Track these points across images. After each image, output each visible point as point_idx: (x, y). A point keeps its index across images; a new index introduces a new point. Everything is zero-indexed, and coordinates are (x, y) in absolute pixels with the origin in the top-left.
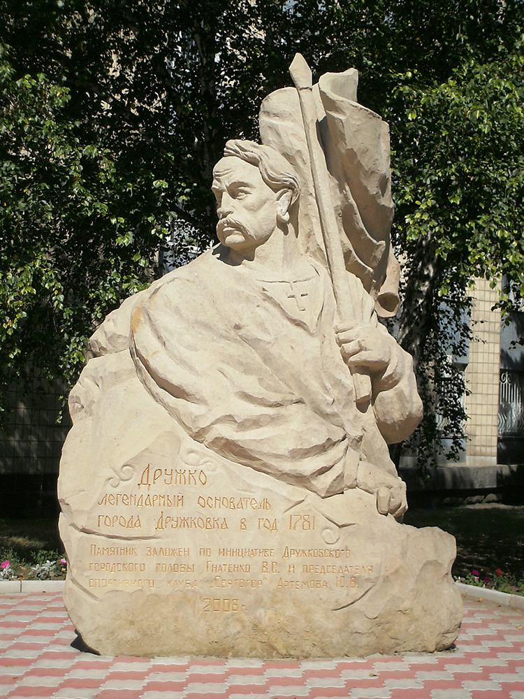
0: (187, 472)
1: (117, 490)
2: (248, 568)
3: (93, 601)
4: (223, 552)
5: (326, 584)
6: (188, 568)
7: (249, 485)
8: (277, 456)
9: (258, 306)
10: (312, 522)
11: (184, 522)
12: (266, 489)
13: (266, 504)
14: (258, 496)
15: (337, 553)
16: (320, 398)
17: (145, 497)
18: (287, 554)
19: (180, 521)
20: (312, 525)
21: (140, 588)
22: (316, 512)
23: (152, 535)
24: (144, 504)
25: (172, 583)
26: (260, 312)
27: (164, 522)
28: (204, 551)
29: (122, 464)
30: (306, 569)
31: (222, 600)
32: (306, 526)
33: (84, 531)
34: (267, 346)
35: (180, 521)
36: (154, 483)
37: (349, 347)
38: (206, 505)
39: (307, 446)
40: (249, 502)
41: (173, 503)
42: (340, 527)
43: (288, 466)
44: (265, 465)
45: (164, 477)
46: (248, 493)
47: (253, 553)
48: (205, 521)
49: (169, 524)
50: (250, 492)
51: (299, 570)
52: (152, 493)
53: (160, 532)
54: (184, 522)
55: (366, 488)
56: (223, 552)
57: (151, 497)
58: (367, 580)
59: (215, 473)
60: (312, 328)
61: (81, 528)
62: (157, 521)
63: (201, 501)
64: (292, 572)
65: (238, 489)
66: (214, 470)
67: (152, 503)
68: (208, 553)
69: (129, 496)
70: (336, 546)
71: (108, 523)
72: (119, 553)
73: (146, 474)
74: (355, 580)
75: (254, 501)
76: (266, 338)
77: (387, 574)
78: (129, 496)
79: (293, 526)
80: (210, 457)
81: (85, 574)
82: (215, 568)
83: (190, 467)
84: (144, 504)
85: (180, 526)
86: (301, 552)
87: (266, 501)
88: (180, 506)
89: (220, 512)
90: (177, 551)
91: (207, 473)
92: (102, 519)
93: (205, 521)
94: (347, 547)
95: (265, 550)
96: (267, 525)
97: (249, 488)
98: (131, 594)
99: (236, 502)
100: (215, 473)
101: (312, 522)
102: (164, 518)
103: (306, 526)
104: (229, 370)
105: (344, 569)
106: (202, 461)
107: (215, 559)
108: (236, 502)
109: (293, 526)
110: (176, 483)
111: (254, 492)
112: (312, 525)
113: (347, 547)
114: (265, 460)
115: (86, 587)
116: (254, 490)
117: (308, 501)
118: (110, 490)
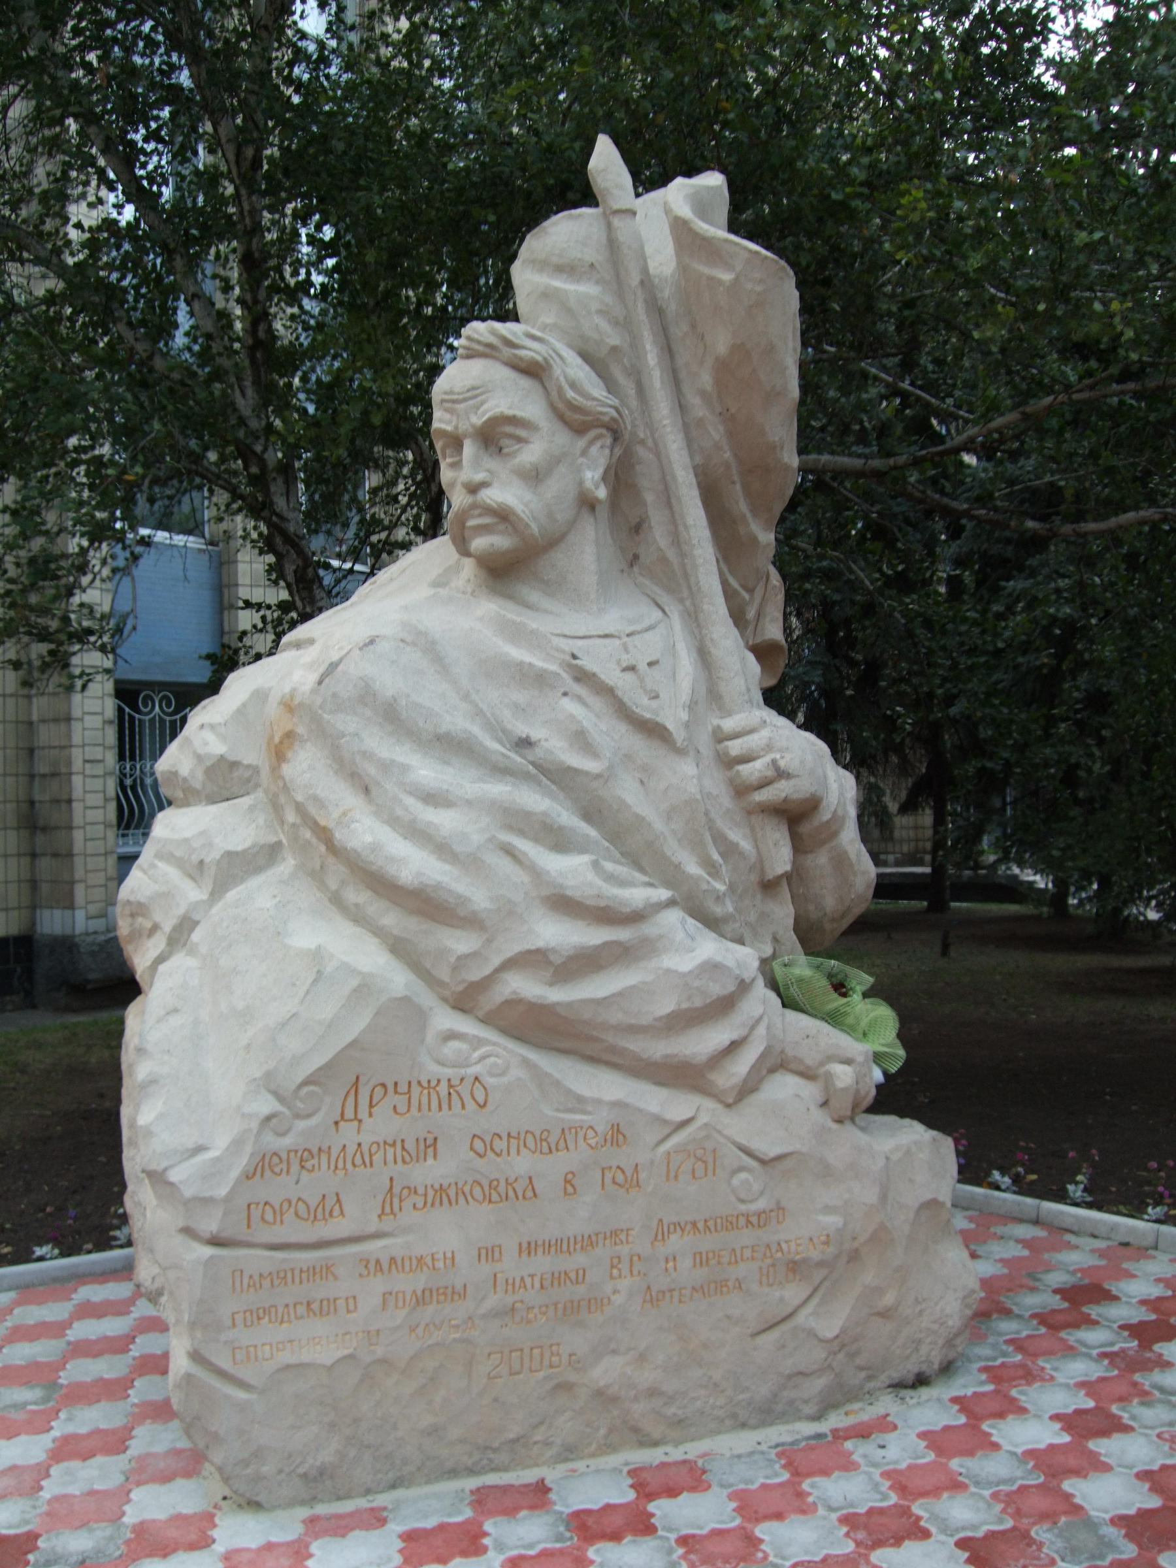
0: (444, 1084)
1: (287, 1141)
2: (580, 1276)
3: (242, 1395)
4: (529, 1248)
5: (739, 1284)
6: (457, 1294)
7: (580, 1099)
8: (634, 1030)
9: (565, 694)
10: (710, 1160)
11: (442, 1195)
12: (618, 1105)
13: (617, 1135)
14: (600, 1120)
15: (759, 1220)
16: (705, 886)
17: (352, 1147)
18: (662, 1232)
19: (431, 1193)
20: (710, 1168)
21: (350, 1351)
22: (722, 1140)
23: (372, 1228)
24: (349, 1165)
25: (420, 1330)
26: (569, 706)
27: (396, 1201)
28: (489, 1253)
29: (299, 1080)
30: (700, 1259)
31: (527, 1351)
32: (700, 1172)
33: (216, 1242)
34: (595, 784)
35: (431, 1193)
36: (371, 1115)
37: (753, 770)
38: (489, 1153)
39: (698, 1002)
40: (581, 1134)
41: (414, 1154)
42: (762, 1162)
43: (658, 1049)
44: (613, 1049)
45: (392, 1099)
46: (578, 1117)
47: (589, 1242)
48: (487, 1189)
49: (408, 1204)
50: (584, 1112)
51: (686, 1263)
52: (366, 1139)
53: (388, 1224)
54: (442, 1195)
55: (802, 1068)
56: (529, 1248)
57: (365, 1148)
58: (821, 1264)
59: (505, 1080)
60: (679, 735)
61: (207, 1235)
62: (380, 1198)
63: (478, 1145)
64: (671, 1269)
65: (558, 1110)
66: (503, 1074)
67: (367, 1161)
68: (497, 1254)
69: (315, 1151)
70: (761, 1204)
71: (269, 1216)
72: (297, 1280)
73: (351, 1099)
74: (795, 1268)
75: (591, 1133)
76: (591, 765)
77: (856, 1244)
78: (315, 1151)
79: (672, 1174)
80: (495, 1044)
81: (223, 1337)
82: (511, 1286)
83: (448, 1072)
84: (349, 1165)
85: (433, 1205)
86: (689, 1227)
87: (616, 1129)
88: (430, 1161)
89: (522, 1164)
90: (429, 1260)
91: (490, 1081)
92: (256, 1213)
93: (487, 1189)
94: (778, 1203)
95: (615, 1233)
96: (620, 1178)
97: (580, 1103)
98: (330, 1368)
99: (553, 1139)
100: (505, 1080)
101: (710, 1160)
102: (396, 1190)
103: (700, 1172)
104: (523, 845)
105: (774, 1247)
106: (477, 1054)
107: (510, 1265)
108: (553, 1139)
109: (672, 1174)
110: (420, 1110)
111: (590, 1113)
112: (710, 1168)
113: (778, 1203)
114: (610, 1038)
115: (225, 1364)
116: (590, 1108)
117: (703, 1119)
118: (272, 1142)
